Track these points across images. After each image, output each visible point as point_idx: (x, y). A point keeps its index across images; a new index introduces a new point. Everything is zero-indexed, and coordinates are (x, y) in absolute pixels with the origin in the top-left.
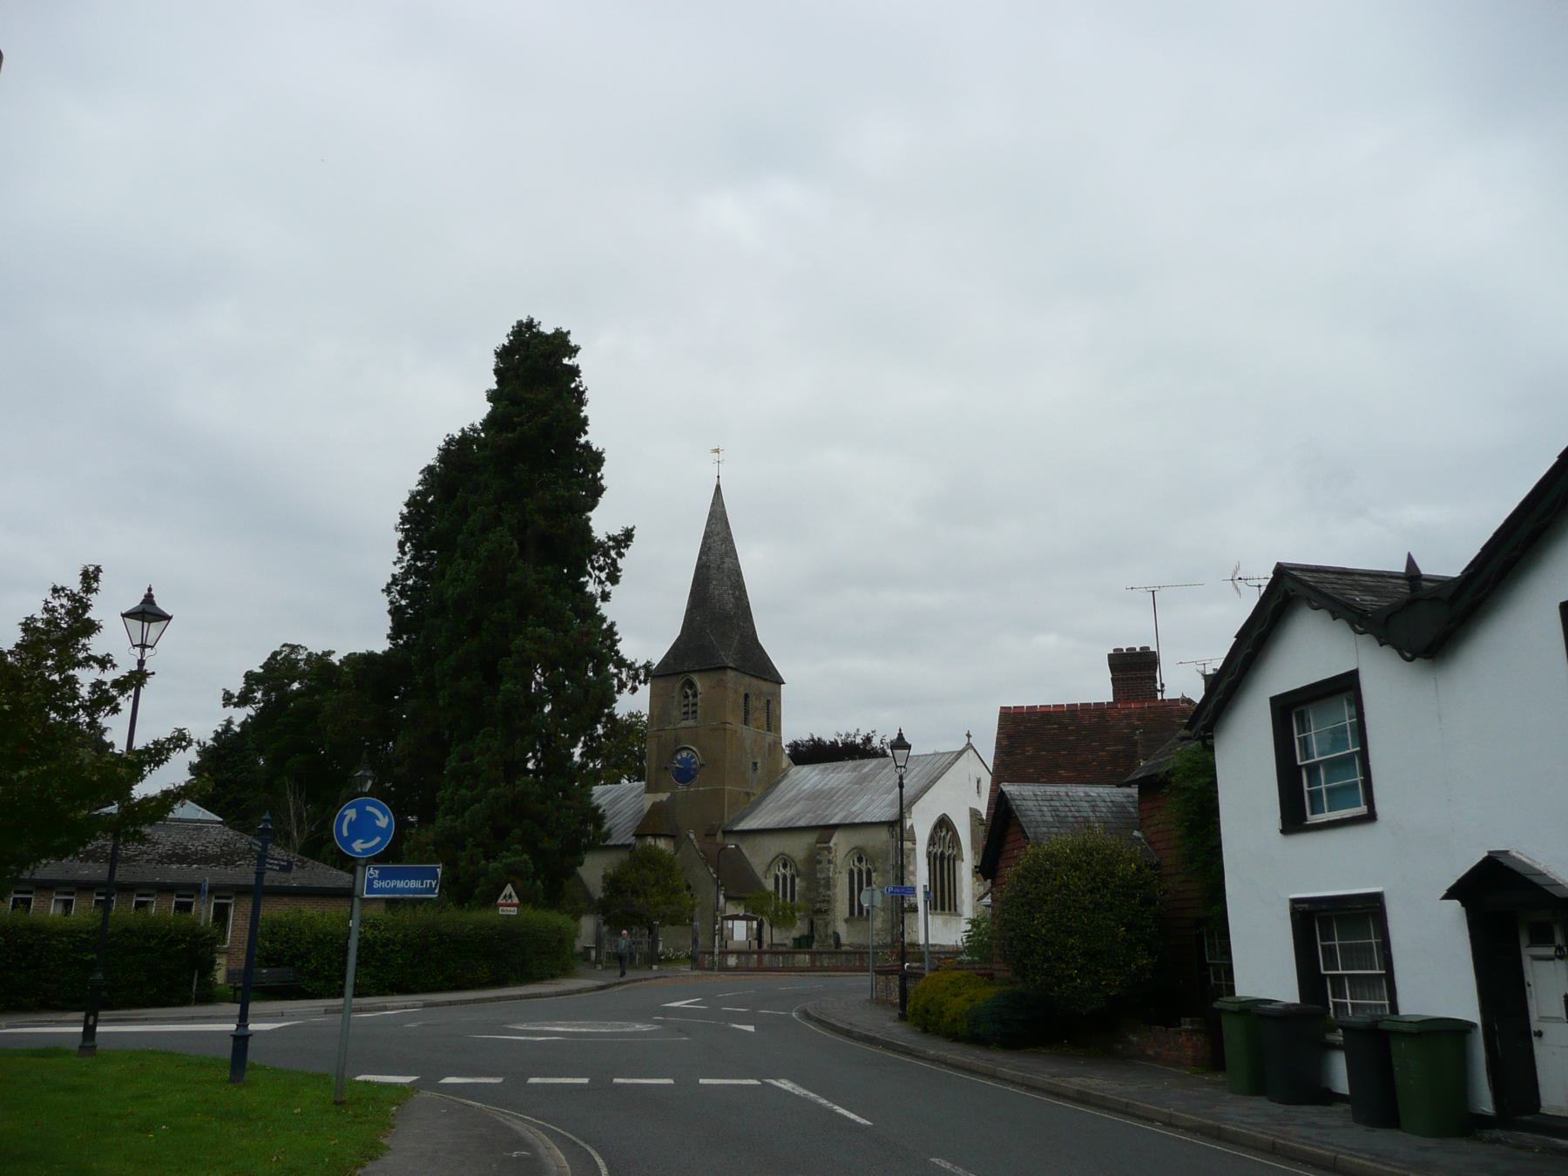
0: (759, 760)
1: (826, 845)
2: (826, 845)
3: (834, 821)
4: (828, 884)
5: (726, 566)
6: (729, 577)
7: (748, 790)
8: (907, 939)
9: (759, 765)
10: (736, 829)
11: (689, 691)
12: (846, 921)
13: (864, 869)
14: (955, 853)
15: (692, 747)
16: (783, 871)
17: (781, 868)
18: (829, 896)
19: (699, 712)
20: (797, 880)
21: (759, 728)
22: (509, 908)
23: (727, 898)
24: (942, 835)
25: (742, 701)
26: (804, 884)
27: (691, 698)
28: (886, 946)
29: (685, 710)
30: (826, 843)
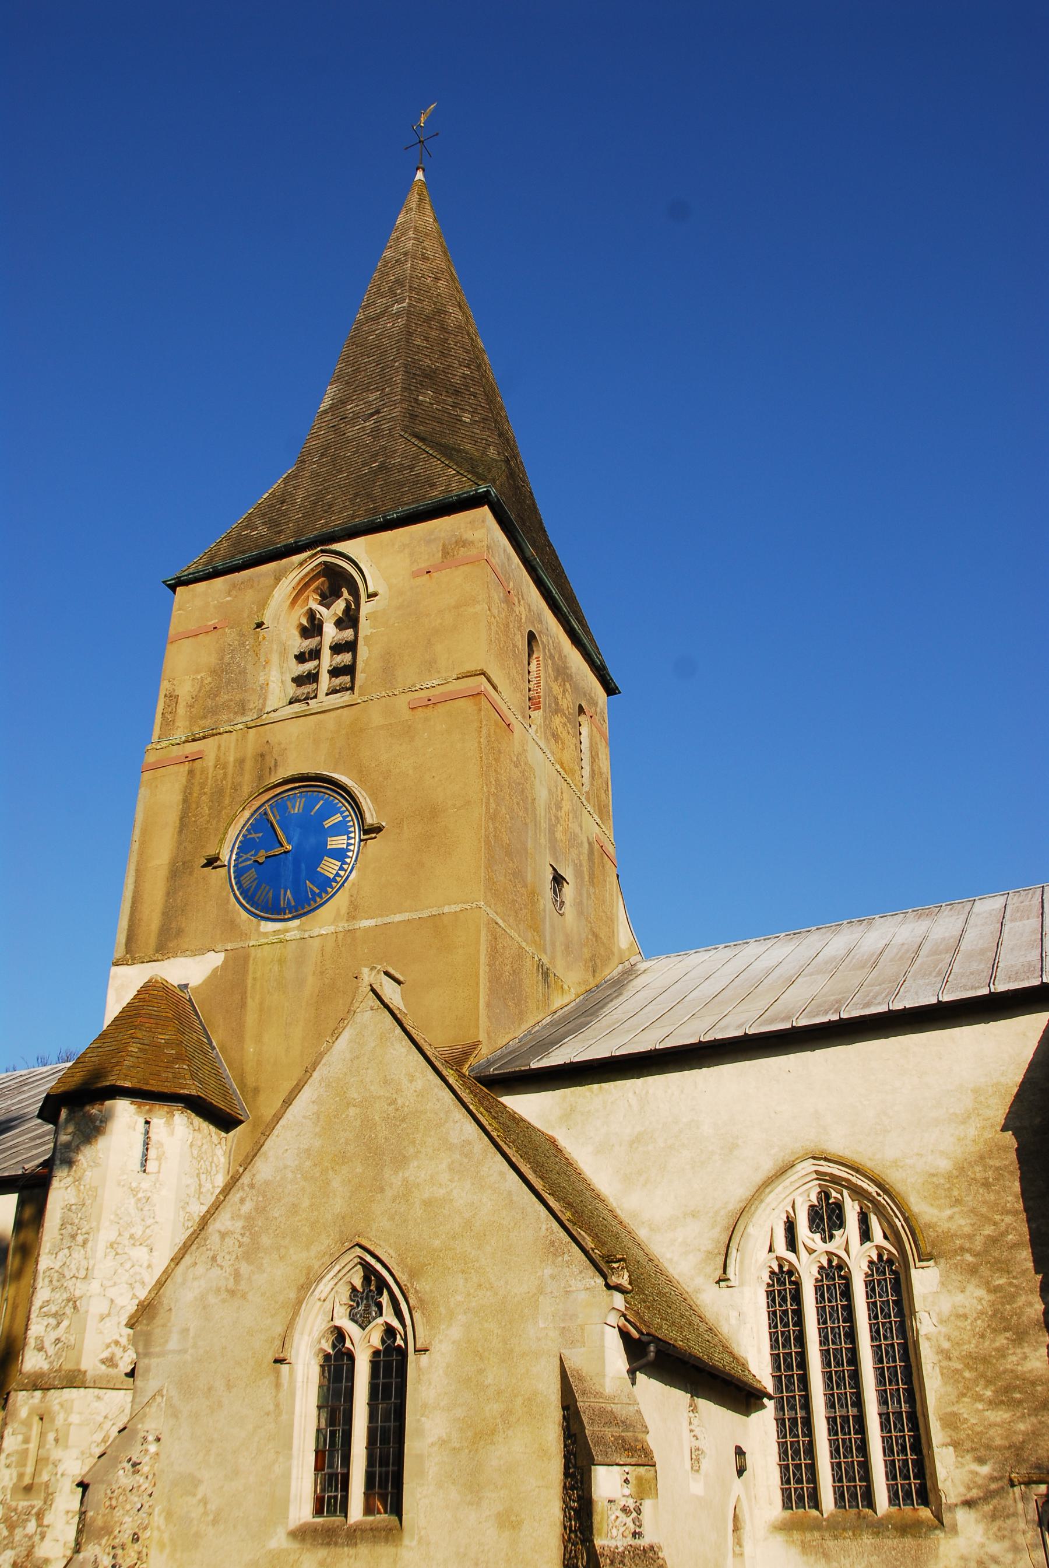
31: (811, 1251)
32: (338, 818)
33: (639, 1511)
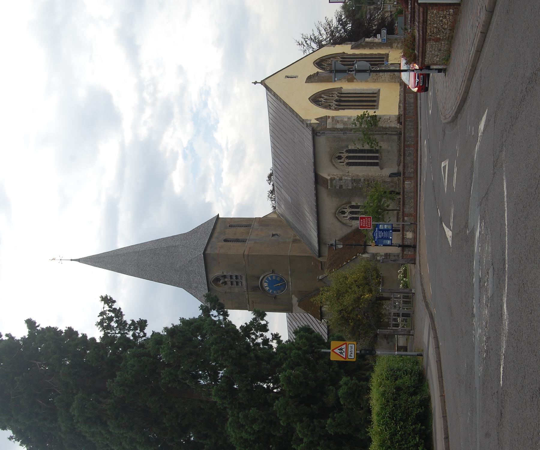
0: (271, 233)
1: (329, 182)
2: (329, 182)
3: (312, 175)
4: (355, 180)
8: (394, 124)
10: (317, 248)
11: (221, 281)
13: (347, 155)
14: (337, 93)
15: (261, 278)
16: (347, 214)
17: (345, 215)
18: (365, 180)
19: (236, 274)
20: (353, 204)
22: (349, 350)
24: (324, 100)
27: (226, 280)
31: (348, 215)
32: (269, 278)
33: (381, 255)
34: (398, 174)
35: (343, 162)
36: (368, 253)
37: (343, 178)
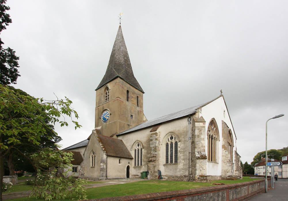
0: (133, 115)
2: (155, 132)
4: (155, 149)
5: (121, 49)
6: (122, 53)
7: (129, 124)
9: (133, 117)
11: (107, 91)
12: (164, 165)
18: (156, 154)
21: (133, 104)
23: (108, 156)
25: (126, 92)
26: (146, 151)
28: (185, 176)
29: (106, 98)
30: (154, 131)
34: (160, 177)
35: (168, 141)
36: (107, 158)
37: (157, 141)
